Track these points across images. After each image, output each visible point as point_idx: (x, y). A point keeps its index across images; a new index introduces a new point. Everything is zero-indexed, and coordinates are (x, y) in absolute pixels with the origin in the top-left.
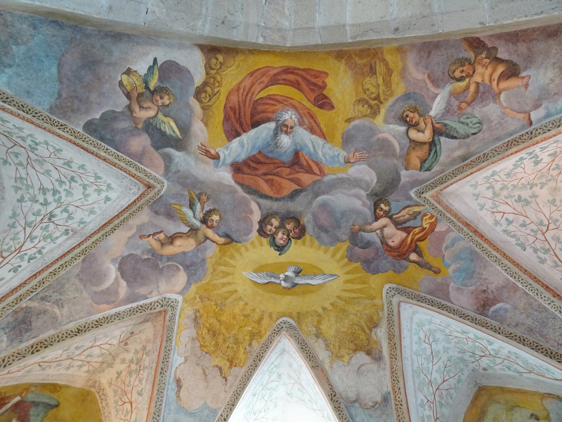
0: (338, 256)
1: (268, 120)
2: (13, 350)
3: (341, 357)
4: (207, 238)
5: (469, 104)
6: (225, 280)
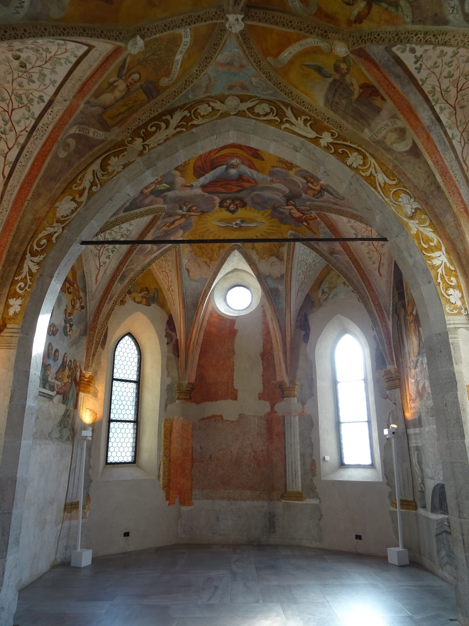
0: (266, 215)
1: (222, 165)
2: (123, 285)
3: (264, 258)
4: (190, 216)
6: (203, 226)
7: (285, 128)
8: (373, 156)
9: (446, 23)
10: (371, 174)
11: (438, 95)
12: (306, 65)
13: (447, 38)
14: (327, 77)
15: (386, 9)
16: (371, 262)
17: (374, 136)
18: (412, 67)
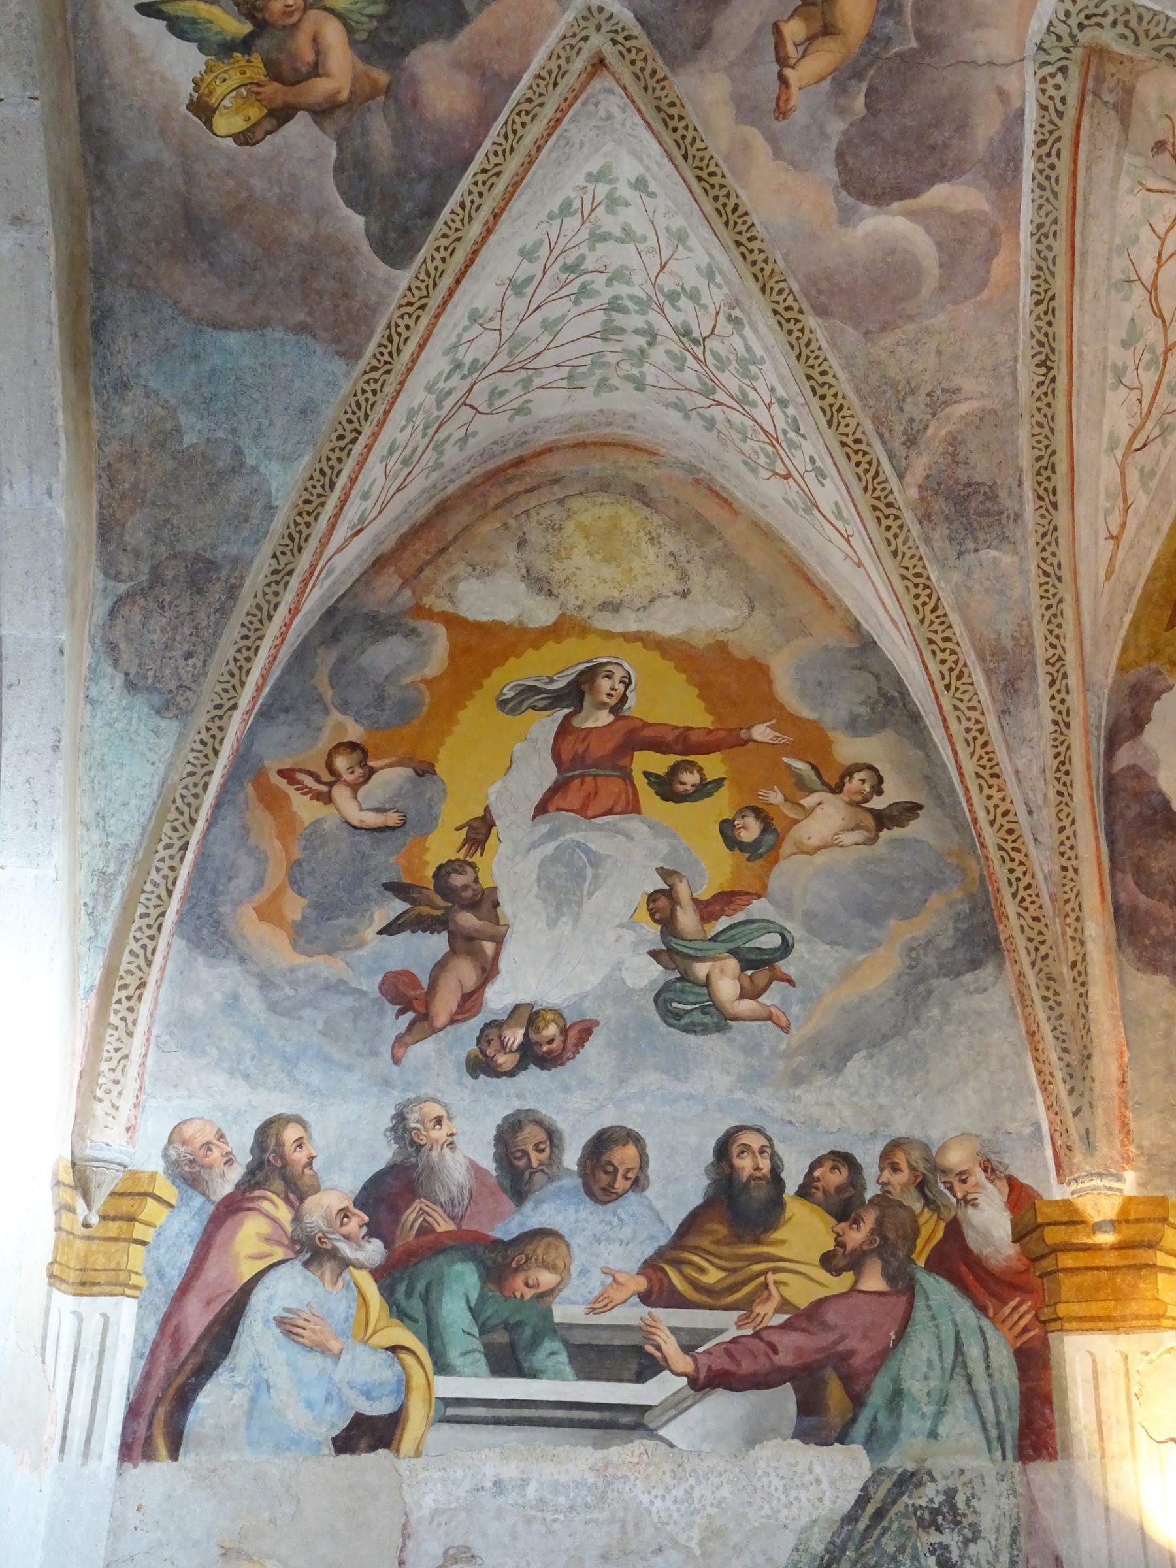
2: (1031, 542)
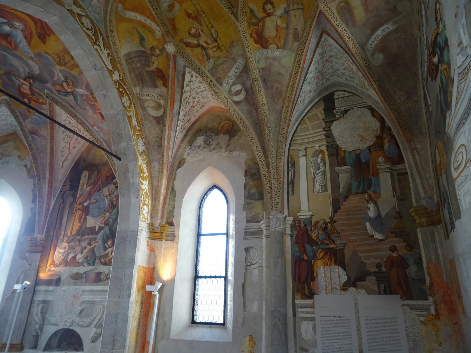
1: (5, 18)
5: (88, 103)
7: (96, 49)
8: (134, 105)
9: (221, 85)
10: (131, 116)
11: (185, 102)
12: (137, 31)
13: (218, 91)
14: (142, 47)
15: (203, 55)
16: (61, 155)
17: (140, 94)
18: (186, 82)
